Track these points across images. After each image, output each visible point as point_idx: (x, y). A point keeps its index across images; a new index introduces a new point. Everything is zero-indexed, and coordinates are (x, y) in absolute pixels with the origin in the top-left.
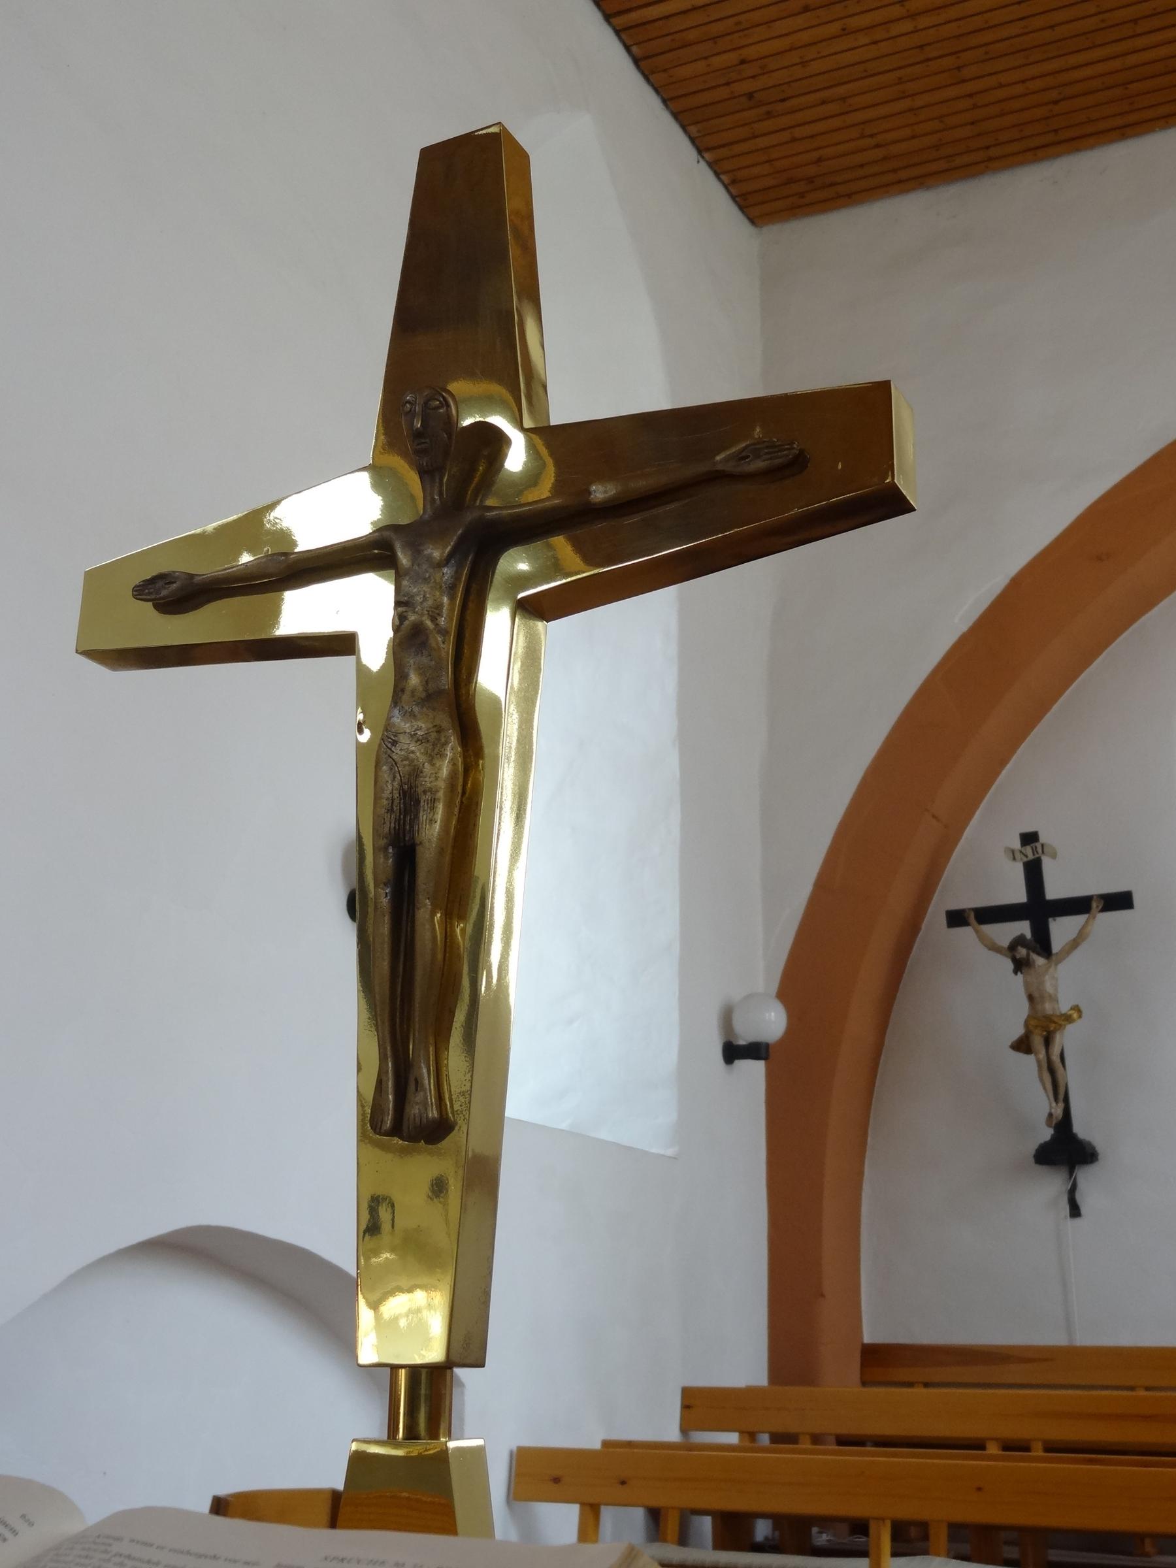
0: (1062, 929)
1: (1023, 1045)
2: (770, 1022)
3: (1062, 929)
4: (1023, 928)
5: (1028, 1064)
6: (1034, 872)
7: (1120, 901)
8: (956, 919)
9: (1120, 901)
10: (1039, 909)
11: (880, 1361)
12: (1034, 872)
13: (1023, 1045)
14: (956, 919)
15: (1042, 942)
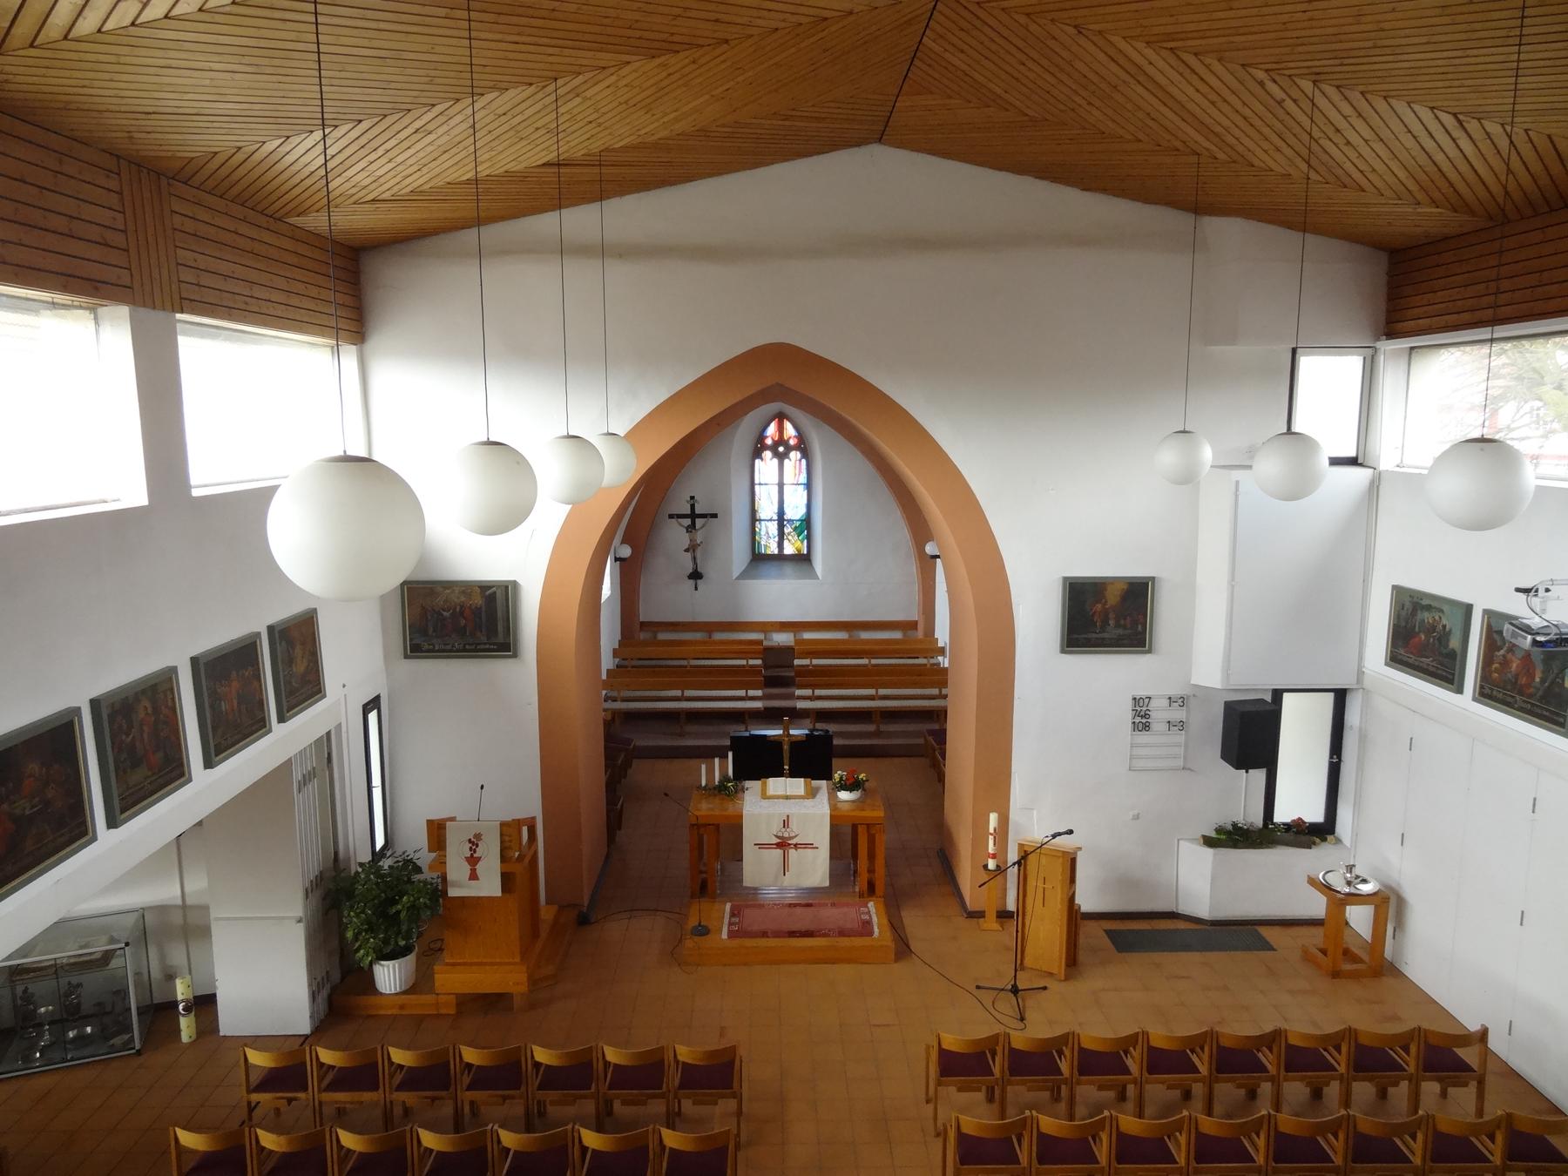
0: (699, 522)
1: (687, 550)
2: (626, 552)
3: (699, 522)
4: (687, 522)
5: (689, 555)
6: (693, 507)
7: (715, 516)
8: (671, 516)
9: (715, 516)
10: (693, 516)
11: (642, 624)
12: (693, 507)
13: (687, 550)
14: (671, 516)
15: (694, 523)
